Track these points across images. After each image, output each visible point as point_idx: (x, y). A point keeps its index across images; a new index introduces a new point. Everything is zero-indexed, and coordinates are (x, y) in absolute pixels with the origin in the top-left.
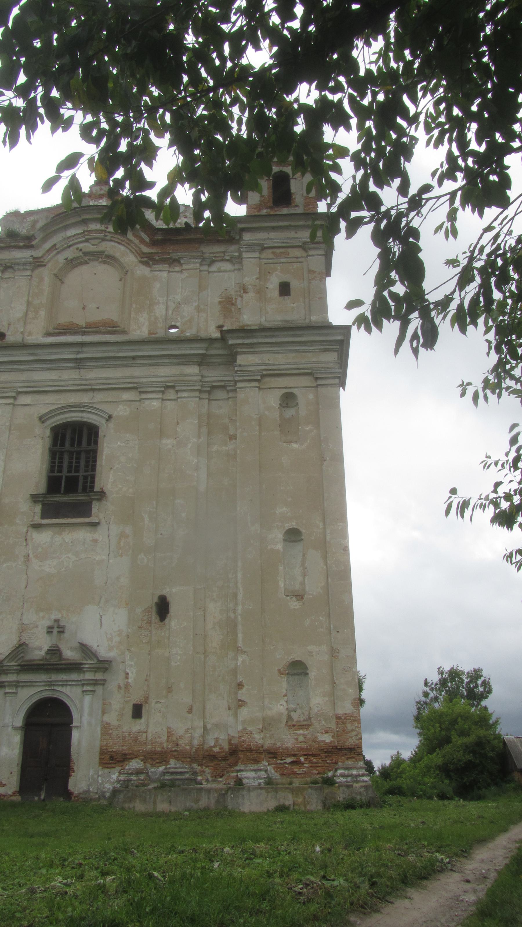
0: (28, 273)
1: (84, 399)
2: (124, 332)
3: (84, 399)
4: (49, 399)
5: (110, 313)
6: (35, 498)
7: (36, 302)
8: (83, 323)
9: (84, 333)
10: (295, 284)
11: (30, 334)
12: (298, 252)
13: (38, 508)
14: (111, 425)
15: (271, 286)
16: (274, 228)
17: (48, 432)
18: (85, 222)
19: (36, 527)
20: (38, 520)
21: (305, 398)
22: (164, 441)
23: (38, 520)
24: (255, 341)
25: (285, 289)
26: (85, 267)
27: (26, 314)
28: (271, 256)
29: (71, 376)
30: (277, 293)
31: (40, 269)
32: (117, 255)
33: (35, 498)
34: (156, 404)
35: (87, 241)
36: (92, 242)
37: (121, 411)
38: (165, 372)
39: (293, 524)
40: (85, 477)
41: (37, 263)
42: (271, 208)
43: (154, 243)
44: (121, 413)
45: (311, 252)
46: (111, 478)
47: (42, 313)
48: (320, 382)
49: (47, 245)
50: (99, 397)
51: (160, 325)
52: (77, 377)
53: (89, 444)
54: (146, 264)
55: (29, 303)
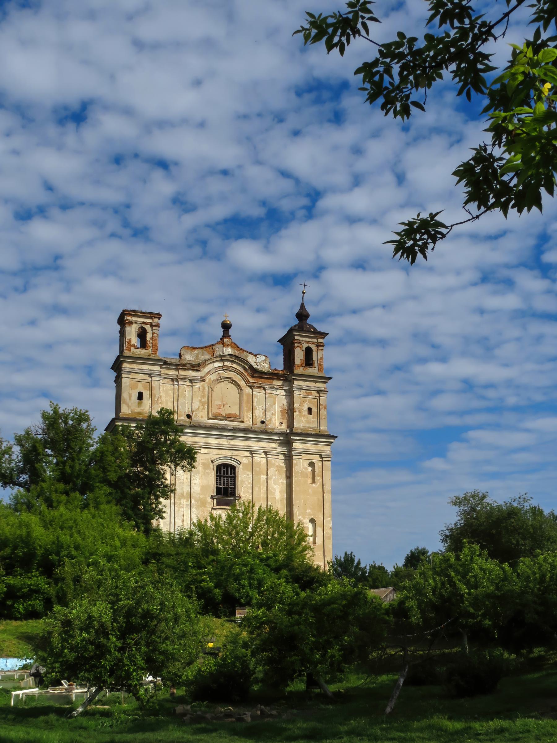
0: (198, 384)
1: (229, 453)
2: (243, 422)
3: (229, 453)
4: (215, 451)
5: (235, 410)
6: (213, 497)
7: (203, 400)
8: (223, 414)
9: (226, 420)
10: (314, 410)
11: (202, 417)
12: (315, 393)
13: (215, 501)
14: (241, 467)
15: (304, 409)
16: (307, 381)
17: (215, 468)
18: (222, 361)
19: (213, 509)
20: (216, 506)
21: (318, 465)
22: (262, 476)
23: (216, 506)
24: (301, 438)
25: (310, 411)
26: (222, 384)
27: (199, 407)
28: (305, 394)
29: (223, 442)
30: (306, 413)
31: (203, 383)
32: (237, 380)
33: (213, 497)
34: (259, 459)
35: (223, 370)
36: (226, 371)
37: (244, 461)
38: (262, 445)
39: (312, 517)
40: (231, 488)
41: (203, 379)
42: (304, 367)
43: (253, 377)
44: (245, 462)
45: (321, 395)
46: (242, 491)
47: (206, 407)
48: (324, 459)
49: (206, 370)
50: (236, 452)
51: (258, 420)
52: (226, 443)
53: (231, 474)
54: (251, 387)
55: (200, 401)
